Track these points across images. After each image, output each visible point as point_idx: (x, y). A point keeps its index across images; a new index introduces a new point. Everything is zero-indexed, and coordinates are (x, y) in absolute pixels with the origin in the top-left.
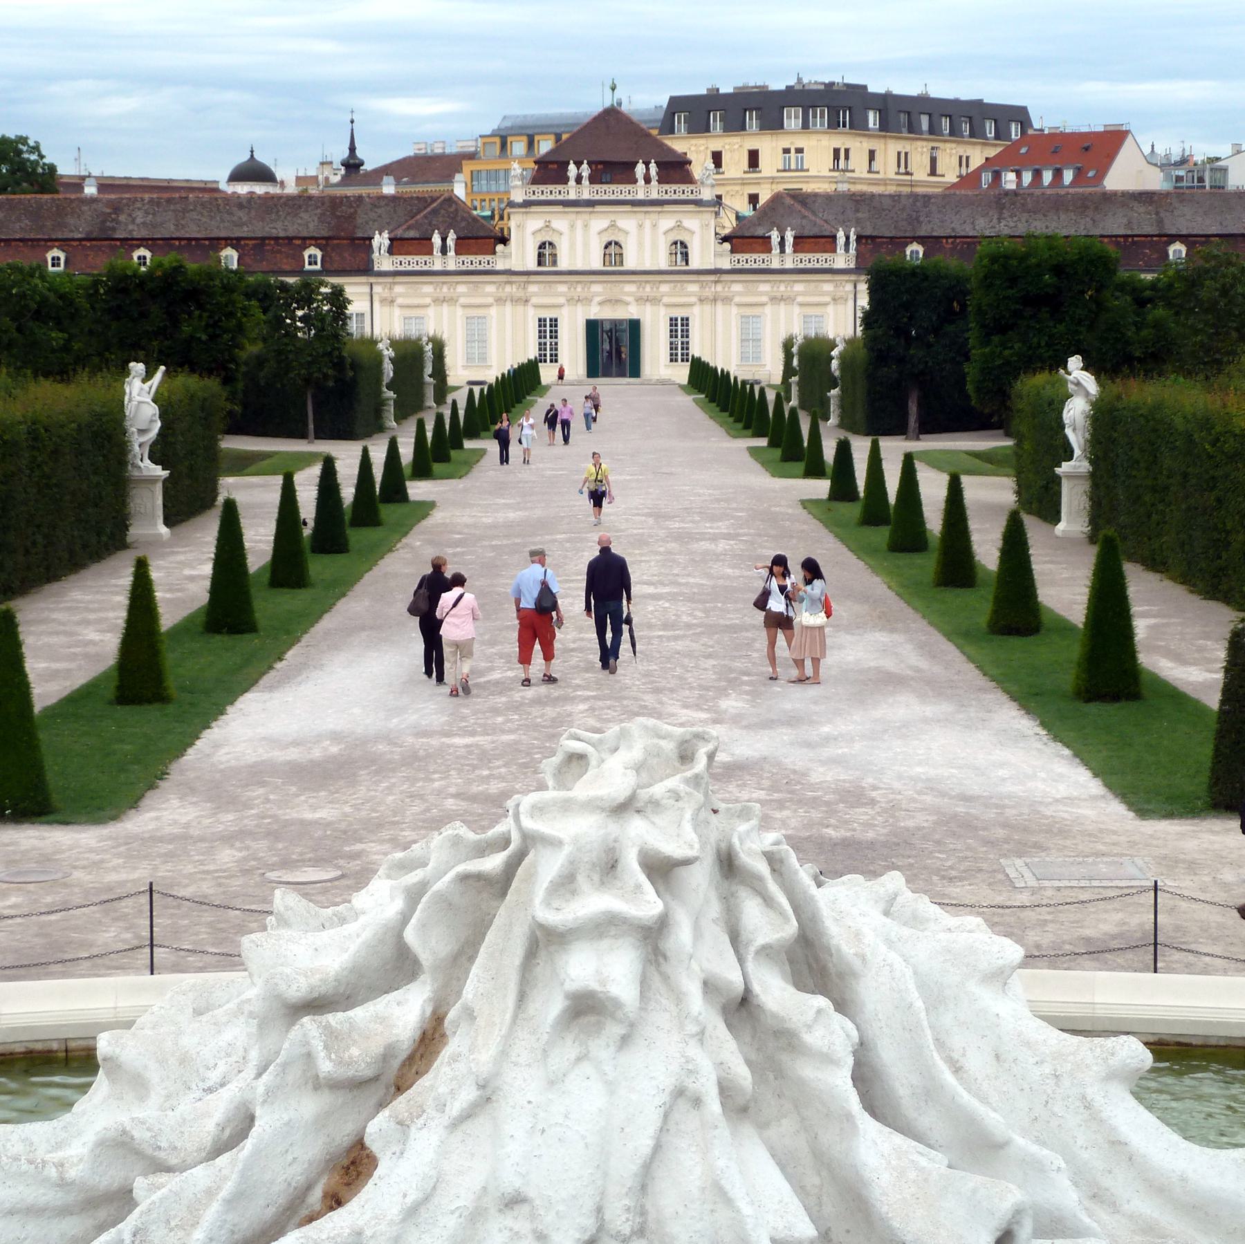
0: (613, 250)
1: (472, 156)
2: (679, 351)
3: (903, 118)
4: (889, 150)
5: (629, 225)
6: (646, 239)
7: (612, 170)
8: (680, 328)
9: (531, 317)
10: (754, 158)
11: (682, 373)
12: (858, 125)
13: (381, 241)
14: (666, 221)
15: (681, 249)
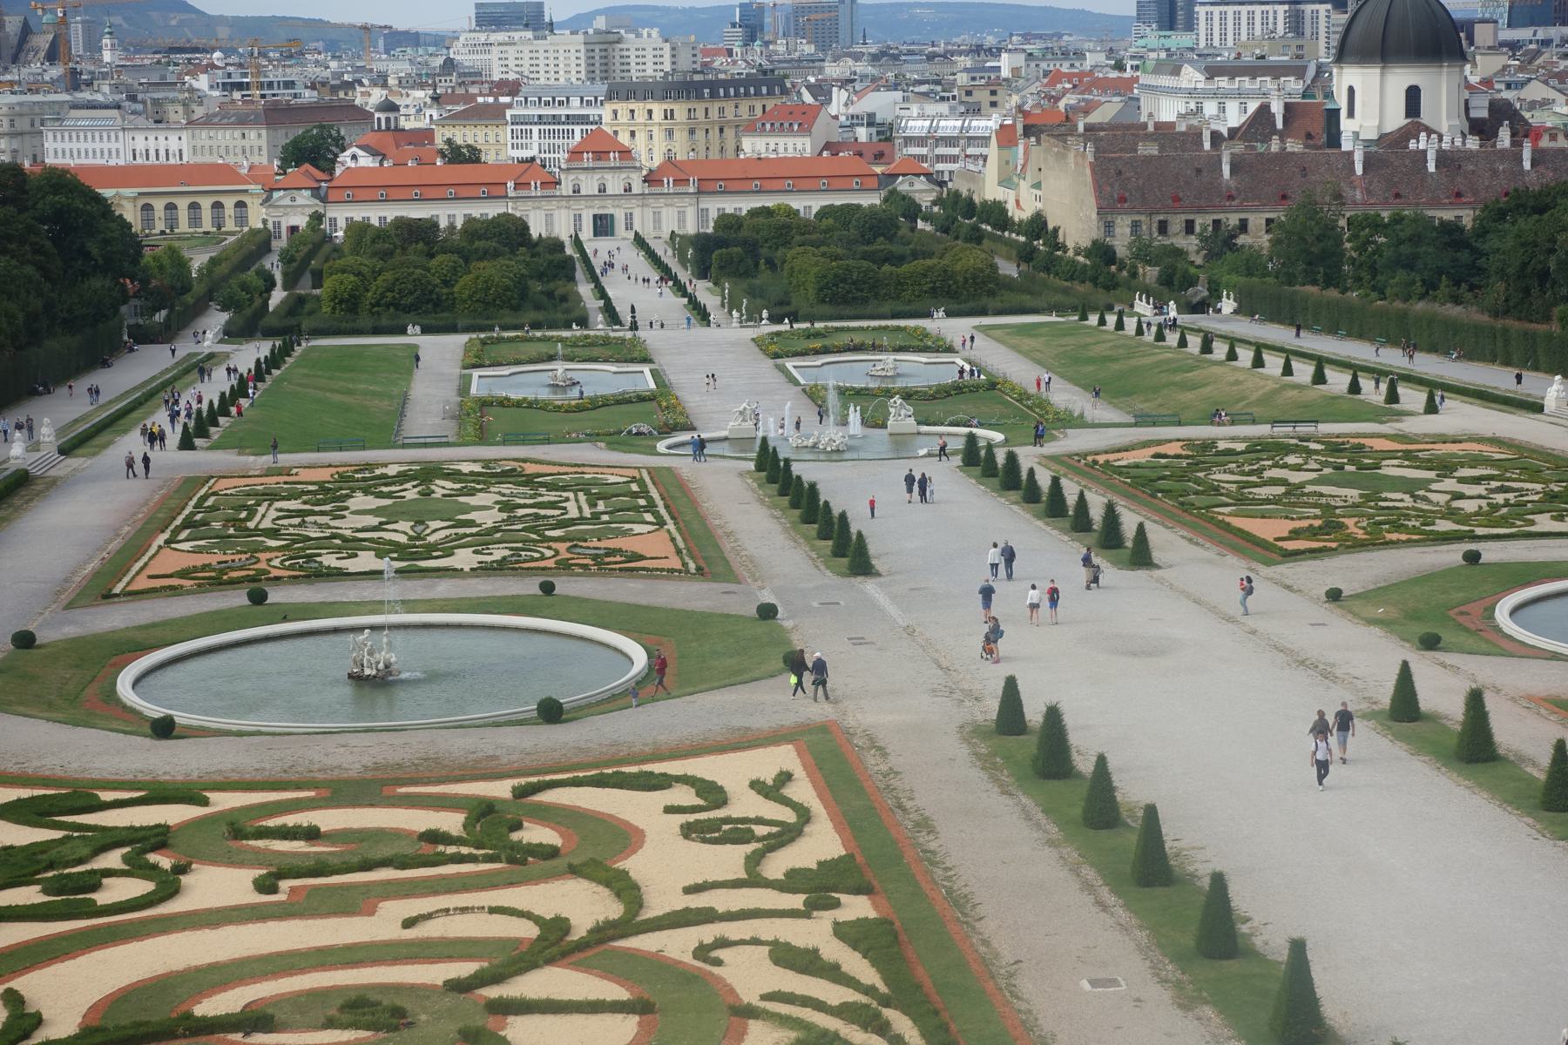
0: (602, 189)
1: (510, 106)
2: (629, 226)
3: (722, 91)
4: (714, 108)
5: (608, 176)
6: (615, 184)
7: (600, 155)
8: (629, 218)
9: (572, 213)
10: (650, 112)
11: (631, 235)
12: (700, 97)
13: (510, 184)
14: (623, 176)
15: (628, 189)
